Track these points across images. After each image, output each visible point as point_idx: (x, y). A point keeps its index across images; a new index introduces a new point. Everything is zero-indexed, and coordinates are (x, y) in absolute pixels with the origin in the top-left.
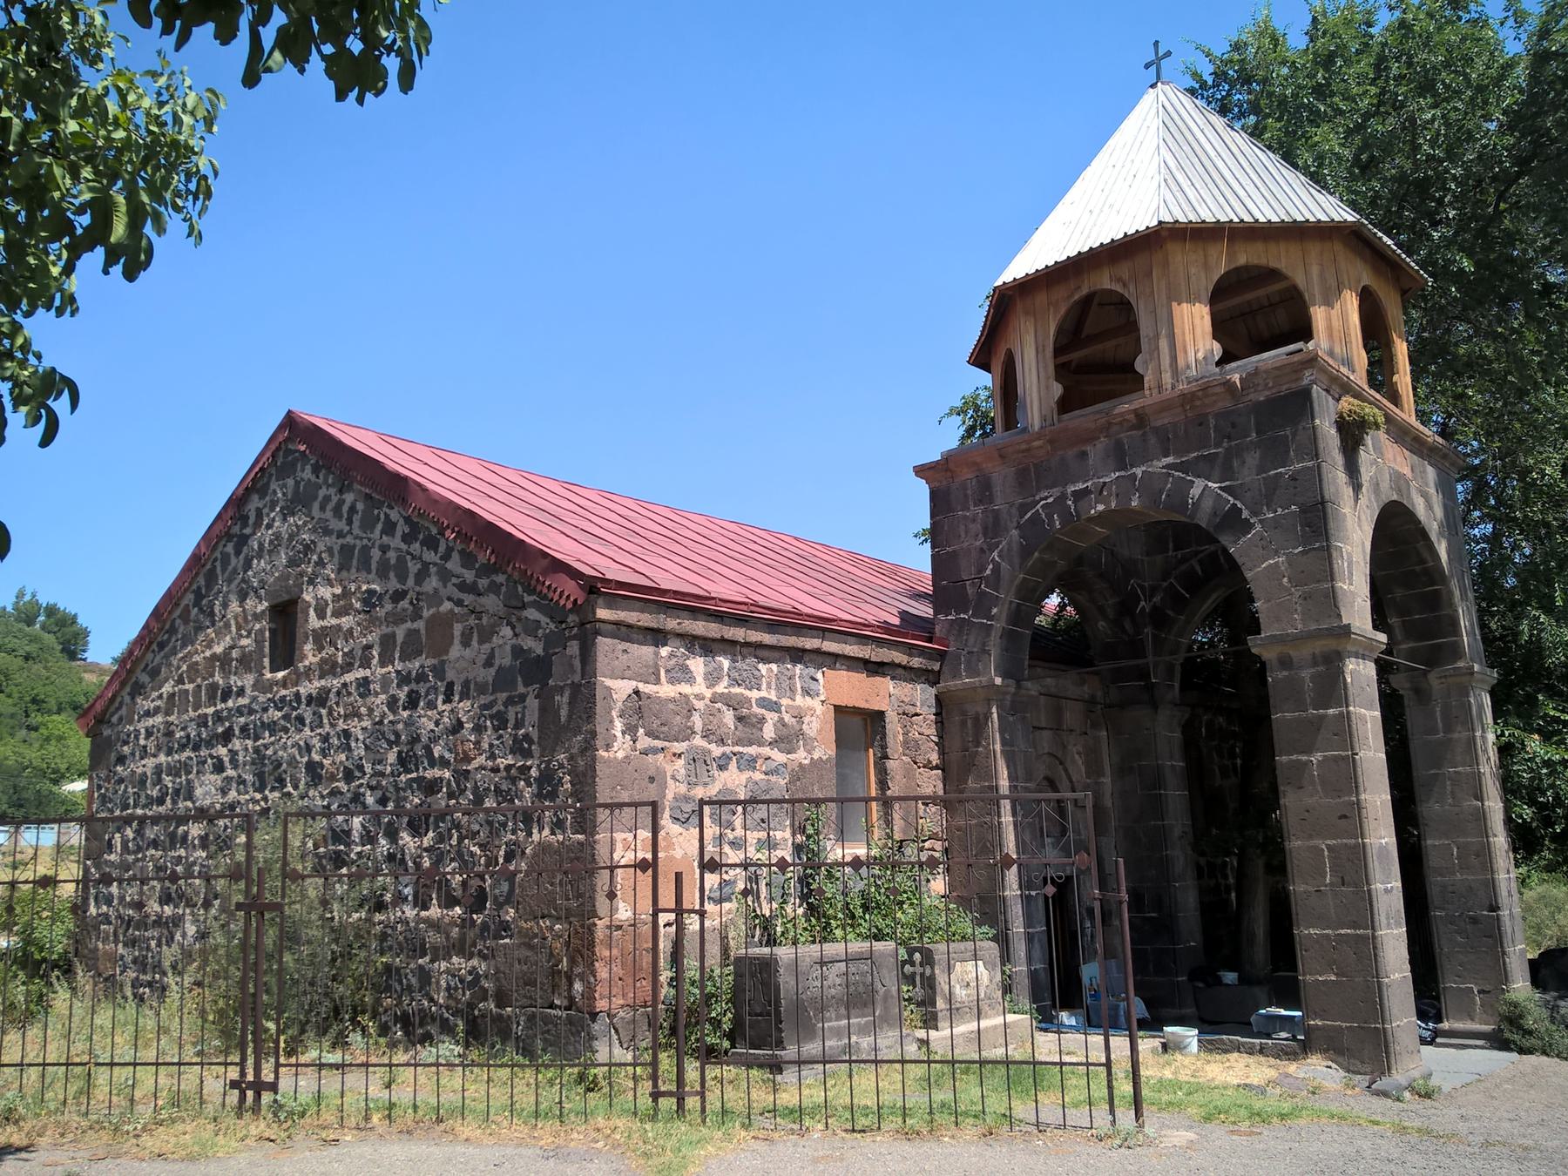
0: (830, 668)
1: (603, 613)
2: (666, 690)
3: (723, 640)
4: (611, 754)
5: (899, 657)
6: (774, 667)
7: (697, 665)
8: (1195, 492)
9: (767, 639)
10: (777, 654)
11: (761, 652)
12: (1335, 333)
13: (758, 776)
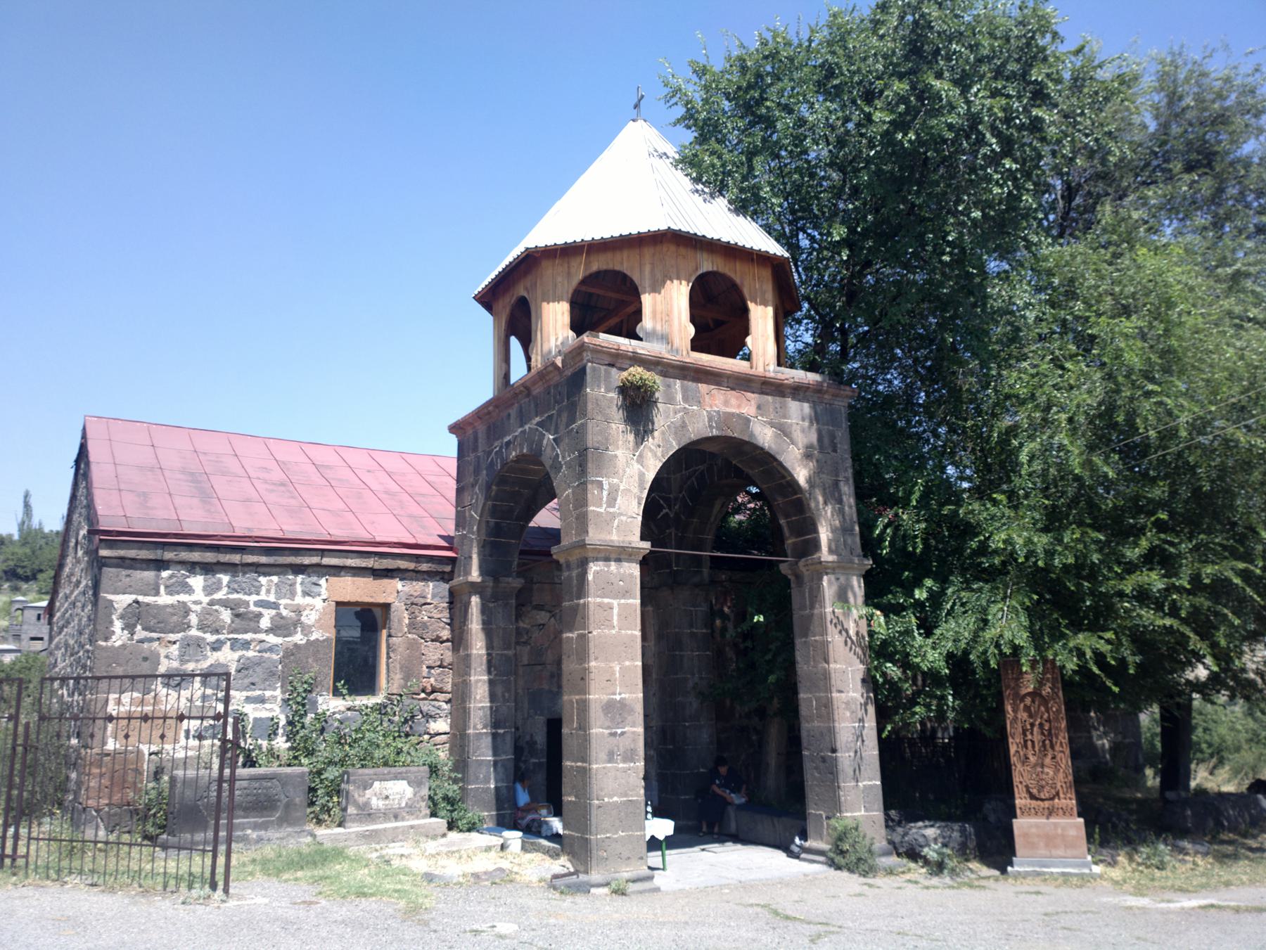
0: (334, 575)
1: (104, 553)
2: (164, 599)
3: (218, 563)
4: (109, 644)
5: (403, 564)
6: (275, 579)
7: (197, 581)
8: (545, 442)
9: (264, 559)
10: (278, 569)
11: (259, 569)
12: (658, 316)
13: (250, 654)
